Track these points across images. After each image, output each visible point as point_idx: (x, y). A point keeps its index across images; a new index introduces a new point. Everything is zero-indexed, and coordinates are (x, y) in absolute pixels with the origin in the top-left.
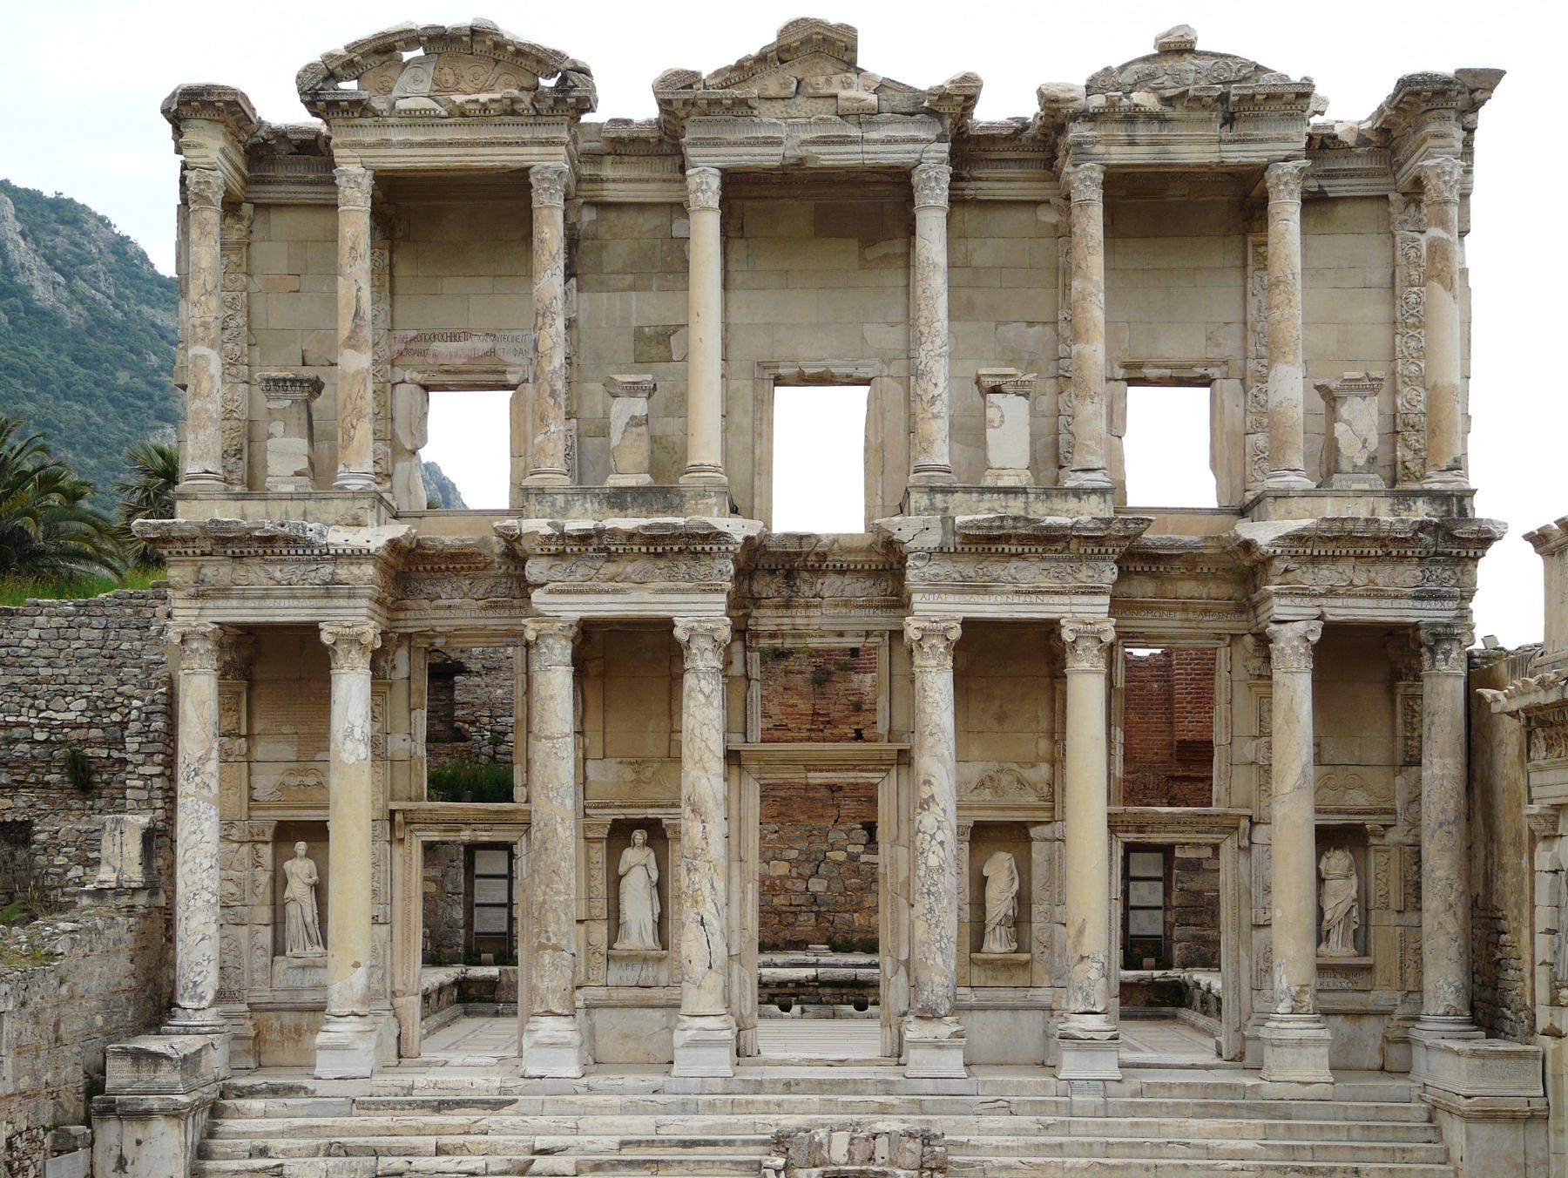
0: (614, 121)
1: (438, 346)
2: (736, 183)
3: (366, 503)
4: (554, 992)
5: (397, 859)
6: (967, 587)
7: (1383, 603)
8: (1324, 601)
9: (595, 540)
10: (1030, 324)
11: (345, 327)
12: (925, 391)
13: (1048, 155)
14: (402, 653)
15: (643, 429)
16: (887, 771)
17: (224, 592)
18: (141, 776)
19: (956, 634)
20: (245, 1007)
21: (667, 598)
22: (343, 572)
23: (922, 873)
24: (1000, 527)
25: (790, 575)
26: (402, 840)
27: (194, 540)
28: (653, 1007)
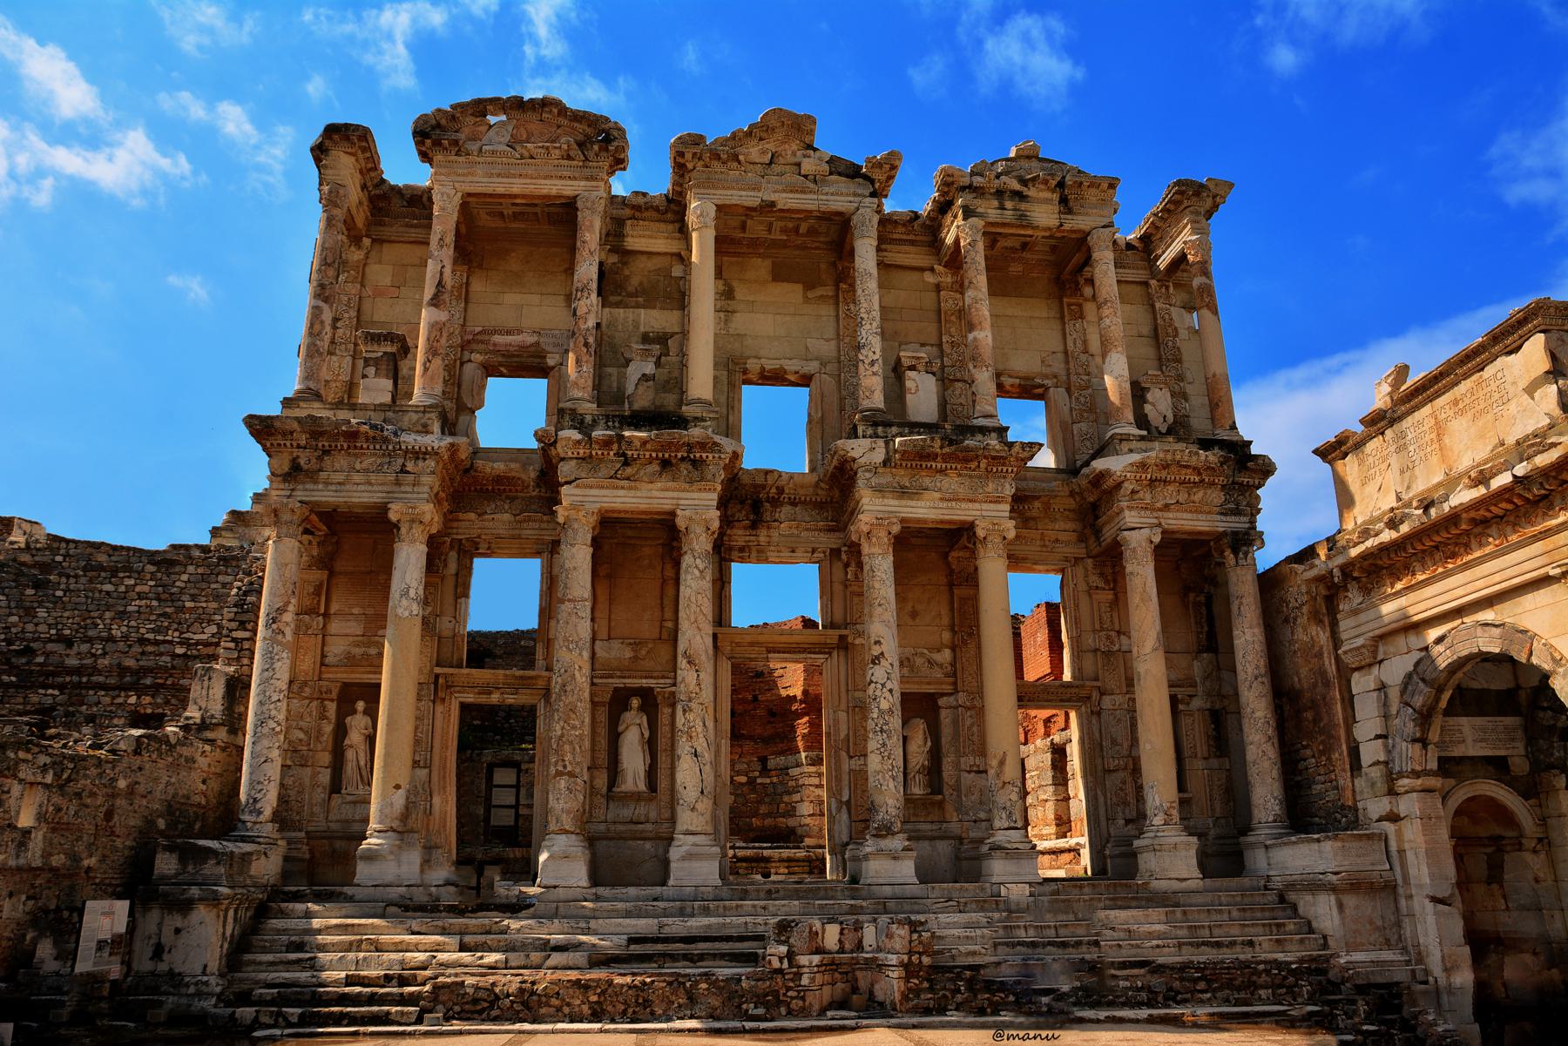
0: (636, 193)
1: (497, 338)
3: (433, 415)
4: (568, 812)
5: (439, 715)
6: (903, 492)
9: (615, 446)
10: (923, 345)
11: (429, 292)
13: (929, 238)
14: (453, 555)
16: (830, 654)
17: (312, 476)
18: (234, 640)
19: (896, 529)
20: (303, 834)
21: (671, 494)
22: (410, 466)
25: (756, 507)
26: (443, 700)
27: (292, 433)
28: (644, 839)
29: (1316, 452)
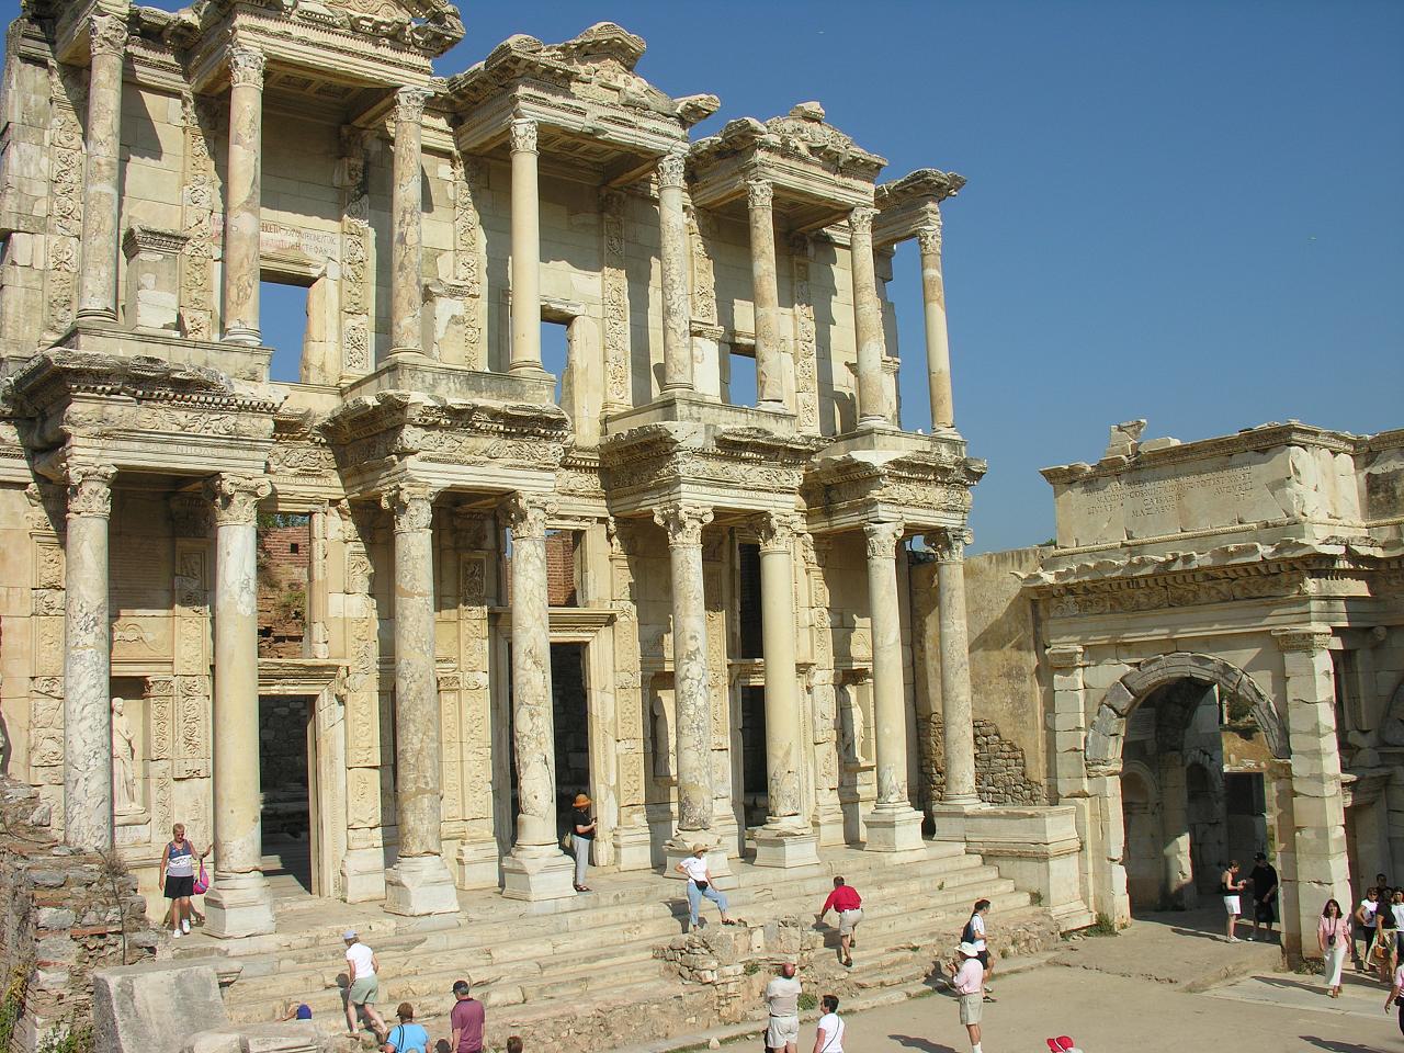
2: (549, 138)
7: (931, 513)
8: (902, 509)
9: (466, 417)
12: (679, 325)
15: (461, 327)
17: (129, 434)
19: (709, 518)
23: (691, 712)
24: (748, 436)
29: (1043, 473)
